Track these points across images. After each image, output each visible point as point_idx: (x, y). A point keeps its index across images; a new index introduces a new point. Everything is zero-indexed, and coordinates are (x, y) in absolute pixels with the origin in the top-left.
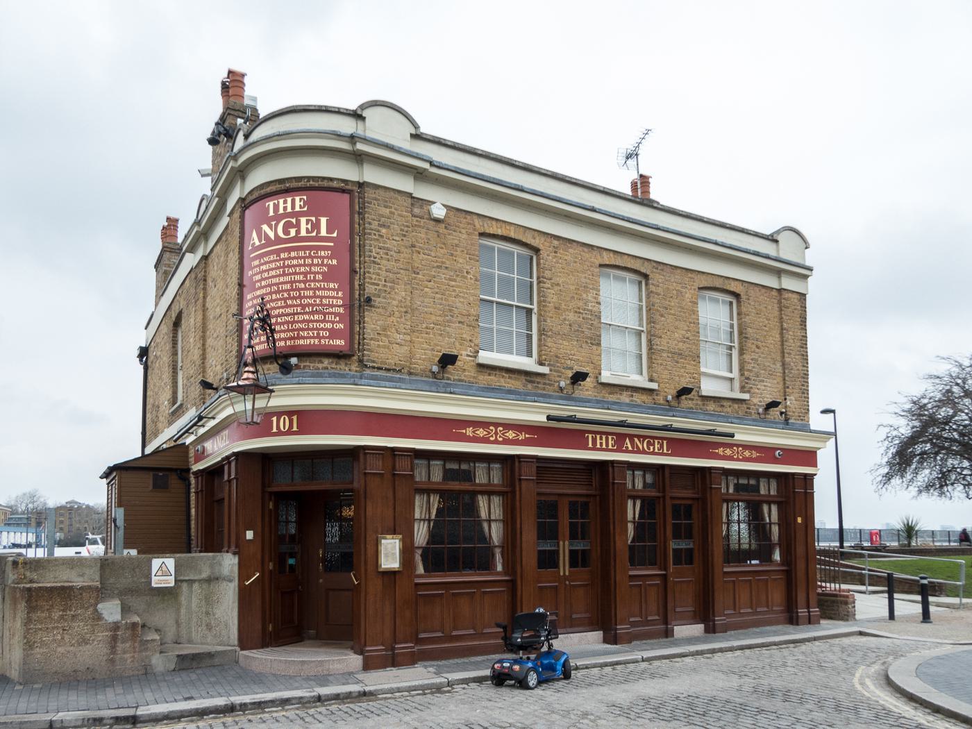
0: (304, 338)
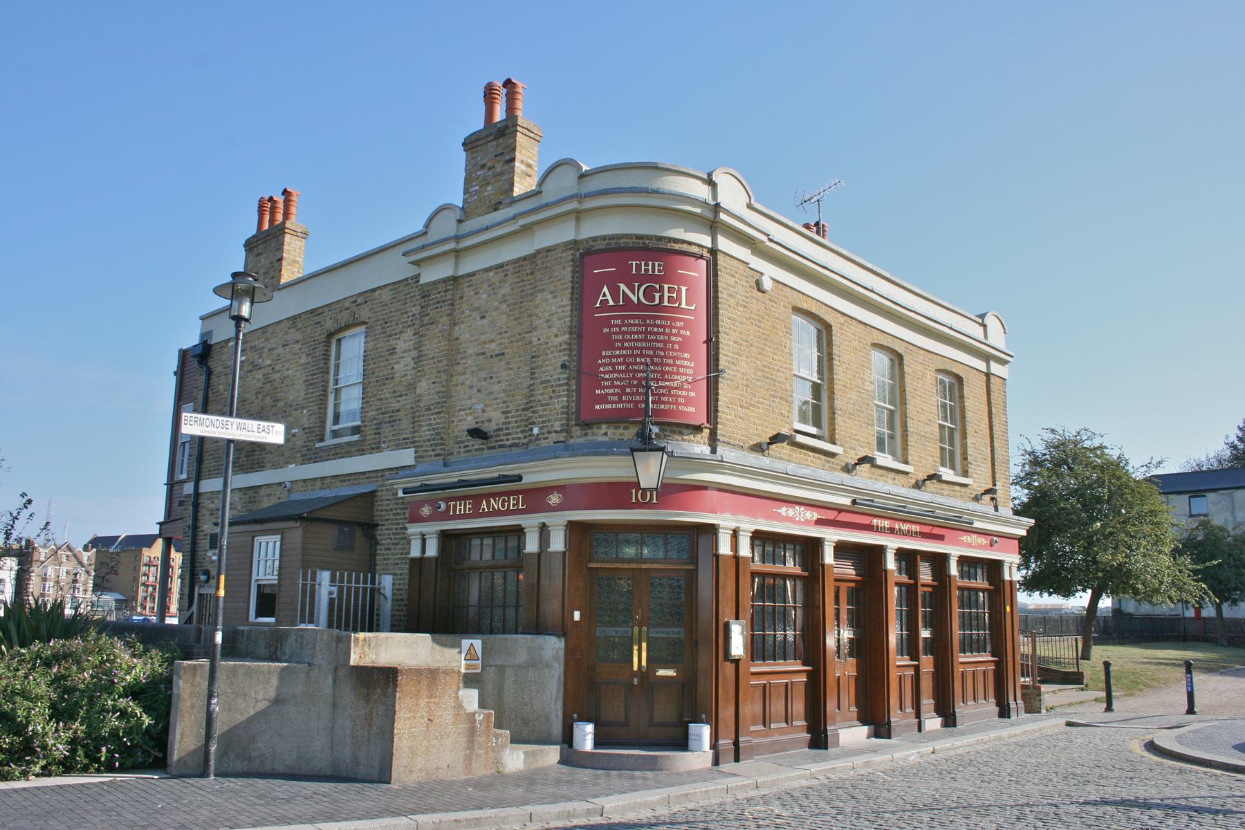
0: (665, 403)
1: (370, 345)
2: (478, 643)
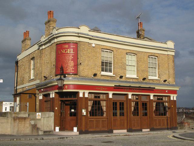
2: (40, 114)
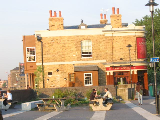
1: (94, 44)
